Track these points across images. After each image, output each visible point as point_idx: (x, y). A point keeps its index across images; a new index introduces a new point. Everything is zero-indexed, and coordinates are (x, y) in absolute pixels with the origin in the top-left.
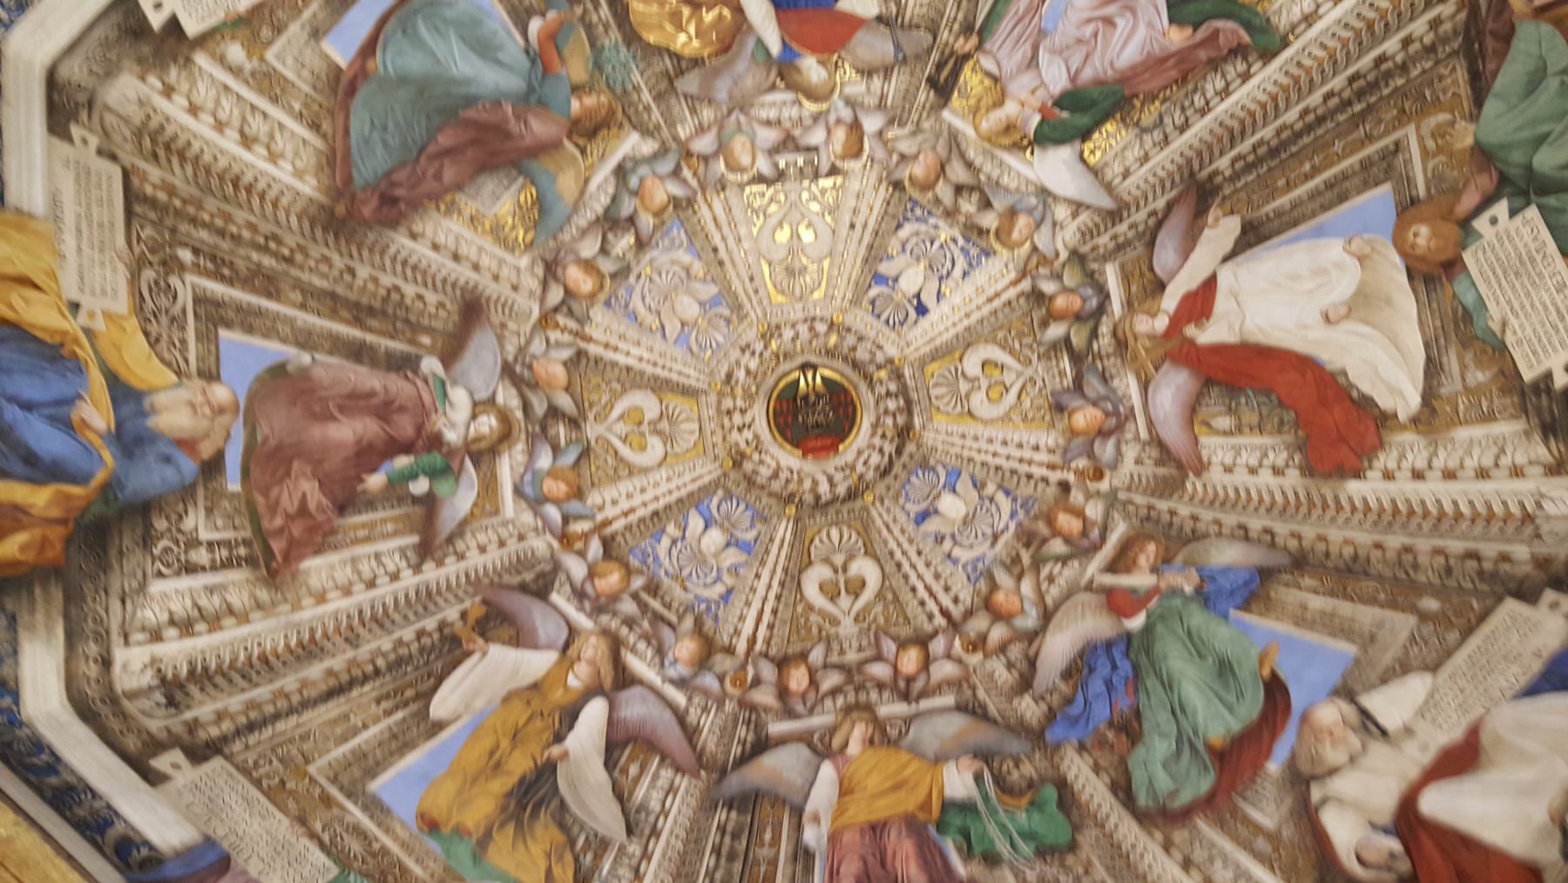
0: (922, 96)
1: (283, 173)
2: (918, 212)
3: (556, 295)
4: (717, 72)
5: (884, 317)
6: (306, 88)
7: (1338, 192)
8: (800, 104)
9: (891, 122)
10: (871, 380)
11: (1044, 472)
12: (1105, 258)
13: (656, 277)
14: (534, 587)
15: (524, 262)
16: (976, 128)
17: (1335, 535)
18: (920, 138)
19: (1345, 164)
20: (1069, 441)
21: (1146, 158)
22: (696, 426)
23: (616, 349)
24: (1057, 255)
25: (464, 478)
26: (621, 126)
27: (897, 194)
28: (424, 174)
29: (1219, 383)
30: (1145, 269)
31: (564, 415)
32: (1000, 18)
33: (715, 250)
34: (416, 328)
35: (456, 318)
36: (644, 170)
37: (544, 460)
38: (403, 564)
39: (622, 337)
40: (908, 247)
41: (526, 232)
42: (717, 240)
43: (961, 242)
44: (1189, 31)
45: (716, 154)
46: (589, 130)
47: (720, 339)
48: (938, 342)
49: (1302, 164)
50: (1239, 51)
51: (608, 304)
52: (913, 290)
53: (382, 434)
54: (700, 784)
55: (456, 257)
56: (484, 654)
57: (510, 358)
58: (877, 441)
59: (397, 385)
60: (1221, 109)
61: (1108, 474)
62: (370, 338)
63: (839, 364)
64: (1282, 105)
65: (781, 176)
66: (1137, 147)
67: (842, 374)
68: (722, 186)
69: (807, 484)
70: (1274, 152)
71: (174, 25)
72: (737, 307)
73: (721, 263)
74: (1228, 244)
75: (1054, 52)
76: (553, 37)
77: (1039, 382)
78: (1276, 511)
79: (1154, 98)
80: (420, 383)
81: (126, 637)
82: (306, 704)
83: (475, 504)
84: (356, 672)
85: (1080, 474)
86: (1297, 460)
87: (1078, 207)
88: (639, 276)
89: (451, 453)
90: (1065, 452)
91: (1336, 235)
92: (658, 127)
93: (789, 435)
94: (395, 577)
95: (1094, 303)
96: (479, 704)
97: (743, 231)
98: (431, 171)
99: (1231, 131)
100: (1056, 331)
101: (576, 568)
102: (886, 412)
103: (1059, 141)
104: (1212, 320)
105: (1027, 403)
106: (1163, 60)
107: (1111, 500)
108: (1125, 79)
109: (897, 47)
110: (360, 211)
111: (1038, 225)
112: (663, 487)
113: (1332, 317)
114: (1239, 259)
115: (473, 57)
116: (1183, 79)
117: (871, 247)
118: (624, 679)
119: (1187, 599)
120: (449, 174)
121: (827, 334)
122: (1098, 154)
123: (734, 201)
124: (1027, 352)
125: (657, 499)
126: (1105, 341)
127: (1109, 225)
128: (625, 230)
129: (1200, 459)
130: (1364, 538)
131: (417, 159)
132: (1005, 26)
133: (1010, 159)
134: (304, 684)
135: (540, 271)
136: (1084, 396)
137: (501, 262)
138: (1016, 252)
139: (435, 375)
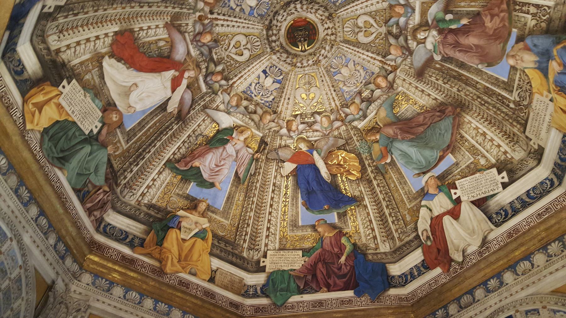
0: (269, 140)
1: (475, 123)
2: (267, 104)
3: (390, 77)
4: (333, 145)
5: (277, 69)
6: (462, 148)
7: (141, 125)
8: (306, 136)
9: (278, 132)
10: (281, 47)
11: (219, 17)
13: (356, 82)
15: (400, 89)
16: (252, 131)
17: (119, 10)
18: (268, 127)
20: (211, 29)
21: (199, 126)
22: (345, 29)
23: (371, 57)
24: (222, 93)
25: (432, 17)
27: (275, 109)
28: (429, 119)
29: (165, 57)
30: (194, 92)
31: (393, 36)
33: (335, 91)
34: (439, 70)
35: (426, 72)
36: (357, 116)
37: (402, 20)
40: (270, 93)
41: (398, 99)
42: (334, 94)
43: (253, 95)
45: (334, 121)
46: (374, 129)
47: (334, 60)
48: (258, 61)
51: (373, 73)
52: (267, 78)
53: (459, 37)
55: (423, 91)
57: (409, 57)
58: (279, 24)
59: (451, 53)
61: (197, 19)
62: (457, 69)
63: (293, 52)
64: (162, 147)
65: (313, 114)
66: (202, 129)
69: (305, 7)
71: (500, 172)
72: (328, 71)
73: (333, 86)
74: (170, 103)
75: (231, 156)
76: (383, 157)
78: (140, 13)
79: (199, 145)
80: (442, 52)
85: (207, 18)
87: (217, 109)
88: (361, 83)
89: (435, 27)
92: (352, 129)
93: (311, 26)
95: (208, 79)
97: (325, 97)
98: (427, 120)
99: (175, 137)
100: (219, 68)
102: (276, 35)
103: (226, 129)
104: (170, 78)
105: (227, 41)
107: (195, 10)
108: (209, 150)
109: (278, 154)
110: (452, 109)
111: (229, 102)
113: (134, 86)
114: (166, 99)
115: (409, 153)
116: (192, 151)
117: (283, 92)
120: (421, 118)
122: (213, 126)
124: (228, 60)
126: (203, 66)
129: (167, 29)
131: (431, 123)
132: (247, 162)
133: (241, 123)
135: (395, 85)
136: (208, 46)
137: (408, 89)
139: (437, 54)
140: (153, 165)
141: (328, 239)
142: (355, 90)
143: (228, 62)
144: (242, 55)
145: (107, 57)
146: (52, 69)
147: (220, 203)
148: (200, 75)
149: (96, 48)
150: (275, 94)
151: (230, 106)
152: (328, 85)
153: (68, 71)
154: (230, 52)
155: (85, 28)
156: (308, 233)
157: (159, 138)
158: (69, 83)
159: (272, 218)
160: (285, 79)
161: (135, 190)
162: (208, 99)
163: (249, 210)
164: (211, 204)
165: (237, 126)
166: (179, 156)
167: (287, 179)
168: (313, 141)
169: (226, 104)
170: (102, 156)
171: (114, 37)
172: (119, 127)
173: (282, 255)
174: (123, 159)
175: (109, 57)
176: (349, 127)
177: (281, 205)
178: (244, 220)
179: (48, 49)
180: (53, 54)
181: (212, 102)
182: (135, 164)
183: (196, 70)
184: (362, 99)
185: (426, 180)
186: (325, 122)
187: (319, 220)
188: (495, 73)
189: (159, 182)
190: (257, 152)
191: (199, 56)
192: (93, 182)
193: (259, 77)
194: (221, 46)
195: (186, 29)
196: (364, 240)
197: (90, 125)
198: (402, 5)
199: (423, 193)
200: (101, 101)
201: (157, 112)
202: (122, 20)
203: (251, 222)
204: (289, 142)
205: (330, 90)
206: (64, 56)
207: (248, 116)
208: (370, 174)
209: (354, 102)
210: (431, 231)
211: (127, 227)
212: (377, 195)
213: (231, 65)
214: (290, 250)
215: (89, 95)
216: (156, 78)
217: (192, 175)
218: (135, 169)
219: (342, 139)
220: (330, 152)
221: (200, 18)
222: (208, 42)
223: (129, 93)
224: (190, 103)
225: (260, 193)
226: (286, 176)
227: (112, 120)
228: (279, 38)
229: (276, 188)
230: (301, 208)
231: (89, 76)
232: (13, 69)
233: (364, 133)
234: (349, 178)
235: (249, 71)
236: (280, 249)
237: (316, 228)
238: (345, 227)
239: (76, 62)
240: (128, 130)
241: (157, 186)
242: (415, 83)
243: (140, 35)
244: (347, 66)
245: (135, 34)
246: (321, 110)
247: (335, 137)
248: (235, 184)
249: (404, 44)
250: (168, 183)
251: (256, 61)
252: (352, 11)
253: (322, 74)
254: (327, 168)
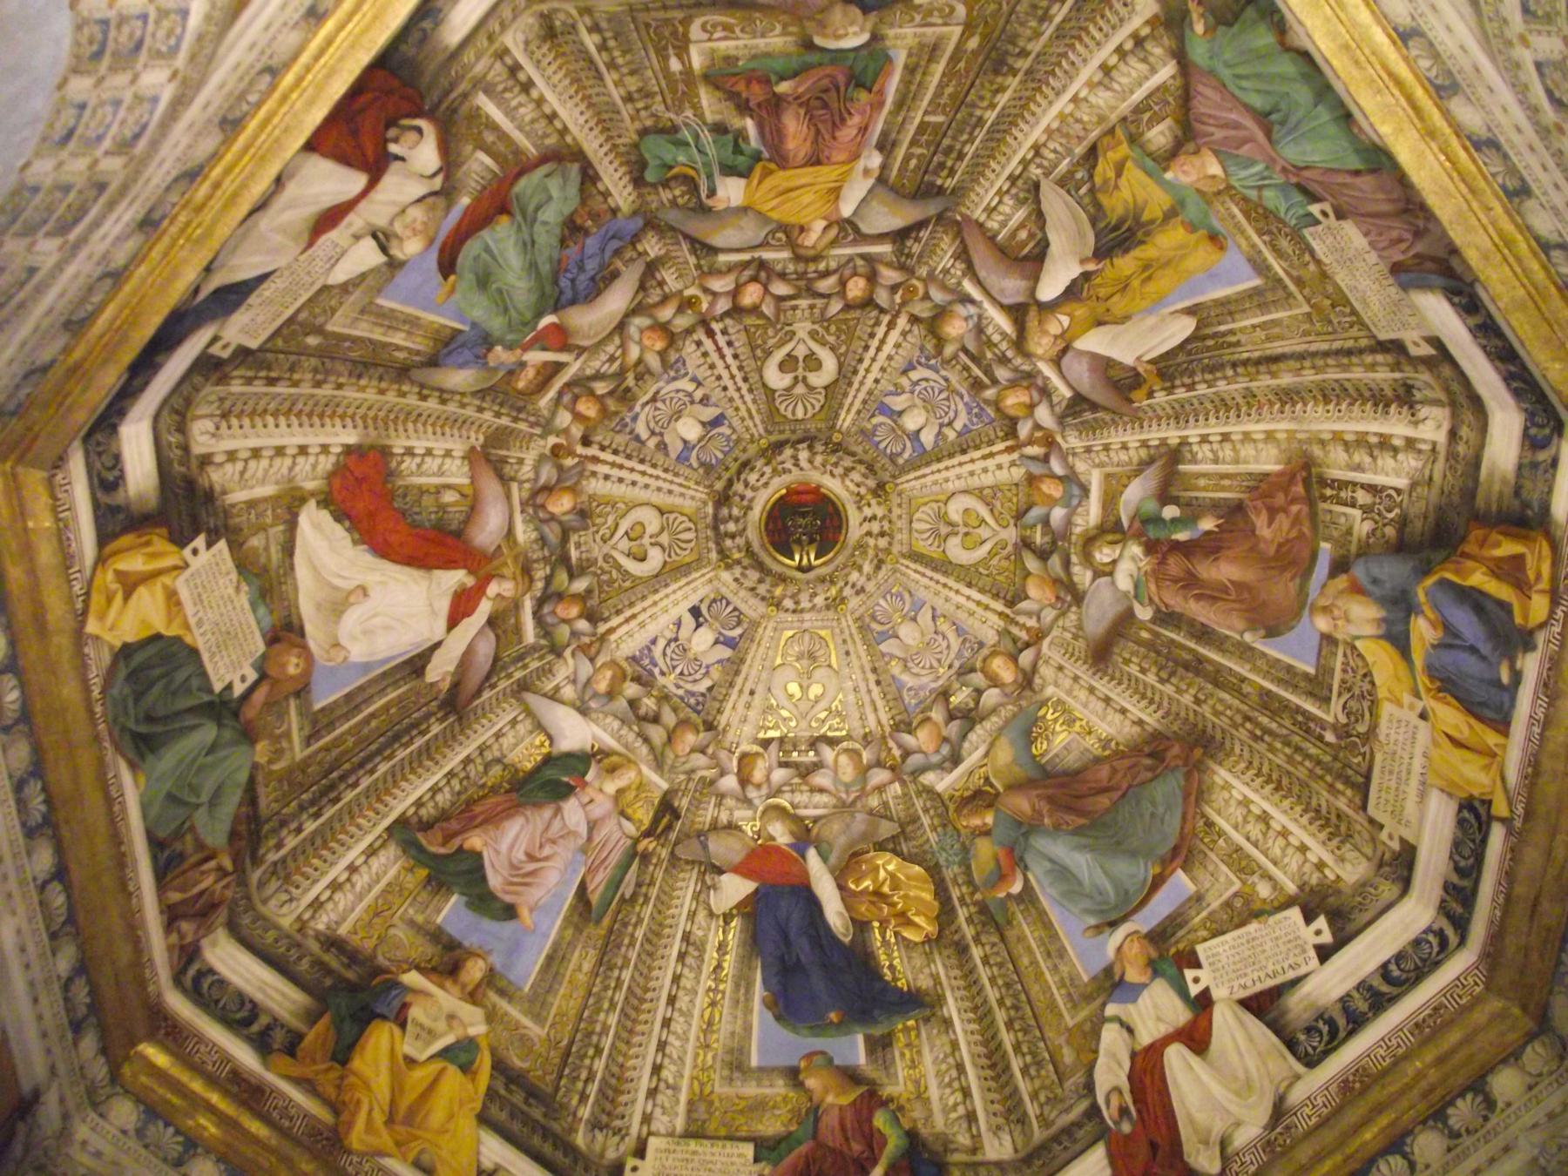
2: (692, 701)
3: (1026, 658)
4: (864, 837)
7: (353, 702)
8: (792, 804)
9: (712, 782)
12: (534, 648)
13: (935, 664)
14: (1086, 406)
15: (1050, 691)
16: (640, 772)
18: (688, 767)
19: (346, 726)
20: (576, 484)
21: (498, 735)
22: (915, 525)
23: (979, 603)
24: (573, 654)
25: (1131, 511)
26: (951, 798)
31: (1034, 552)
32: (617, 866)
33: (878, 683)
34: (1150, 646)
35: (1116, 650)
36: (935, 759)
37: (1058, 514)
38: (1195, 448)
39: (972, 614)
40: (703, 671)
41: (1044, 717)
42: (876, 690)
43: (656, 671)
44: (467, 846)
45: (870, 767)
46: (979, 798)
47: (882, 602)
48: (683, 581)
49: (378, 728)
50: (426, 826)
51: (981, 645)
52: (701, 630)
54: (963, 210)
55: (1107, 700)
56: (1138, 359)
57: (1074, 609)
59: (1176, 601)
60: (437, 777)
61: (547, 452)
63: (776, 568)
64: (389, 778)
65: (814, 743)
67: (775, 559)
68: (867, 739)
70: (397, 737)
72: (863, 628)
73: (874, 670)
75: (572, 834)
80: (1156, 599)
81: (1434, 450)
82: (1301, 357)
83: (1126, 486)
84: (1252, 369)
87: (554, 696)
88: (950, 667)
89: (1139, 536)
92: (919, 794)
94: (1204, 439)
95: (546, 609)
96: (1151, 320)
97: (851, 698)
98: (1119, 776)
99: (430, 758)
100: (580, 585)
101: (1043, 415)
103: (569, 755)
106: (486, 821)
109: (705, 847)
111: (589, 681)
112: (953, 474)
113: (360, 592)
116: (470, 803)
117: (737, 673)
118: (1017, 312)
119: (500, 341)
121: (784, 597)
122: (537, 742)
123: (857, 724)
124: (606, 566)
125: (961, 464)
128: (956, 708)
130: (350, 394)
132: (615, 858)
133: (611, 743)
134: (1298, 372)
135: (1037, 681)
137: (1069, 692)
140: (359, 827)
141: (836, 1112)
142: (934, 685)
143: (604, 572)
144: (643, 560)
145: (312, 503)
147: (527, 970)
148: (528, 596)
150: (716, 674)
152: (862, 668)
153: (216, 514)
154: (614, 547)
155: (282, 420)
156: (776, 1090)
158: (209, 545)
159: (672, 1039)
160: (749, 636)
161: (297, 887)
162: (534, 665)
163: (606, 1005)
164: (498, 967)
165: (600, 751)
166: (432, 811)
167: (726, 923)
168: (808, 818)
169: (580, 686)
170: (237, 764)
172: (297, 694)
173: (694, 1153)
174: (286, 787)
176: (912, 787)
177: (701, 1000)
178: (589, 1034)
179: (186, 448)
180: (194, 464)
182: (312, 810)
184: (949, 711)
185: (1118, 943)
186: (847, 771)
187: (809, 1056)
188: (1285, 652)
189: (366, 878)
190: (647, 834)
192: (201, 830)
193: (679, 624)
196: (939, 1122)
198: (1059, 478)
199: (1112, 984)
202: (370, 422)
203: (607, 1043)
204: (741, 814)
205: (866, 680)
206: (217, 477)
207: (635, 728)
208: (964, 925)
209: (928, 719)
210: (1132, 1092)
211: (260, 989)
212: (981, 989)
213: (611, 582)
214: (718, 1138)
217: (459, 874)
218: (310, 826)
219: (891, 819)
220: (855, 855)
222: (565, 514)
224: (487, 667)
225: (644, 957)
226: (725, 915)
228: (744, 529)
229: (691, 949)
230: (759, 1015)
232: (99, 475)
233: (952, 807)
234: (905, 934)
235: (655, 603)
236: (689, 1135)
237: (801, 1077)
238: (885, 1080)
239: (238, 496)
240: (317, 706)
241: (358, 888)
242: (1087, 677)
244: (914, 619)
246: (837, 734)
247: (871, 813)
248: (576, 919)
249: (1062, 574)
250: (389, 884)
251: (676, 580)
252: (935, 483)
253: (846, 635)
254: (843, 899)
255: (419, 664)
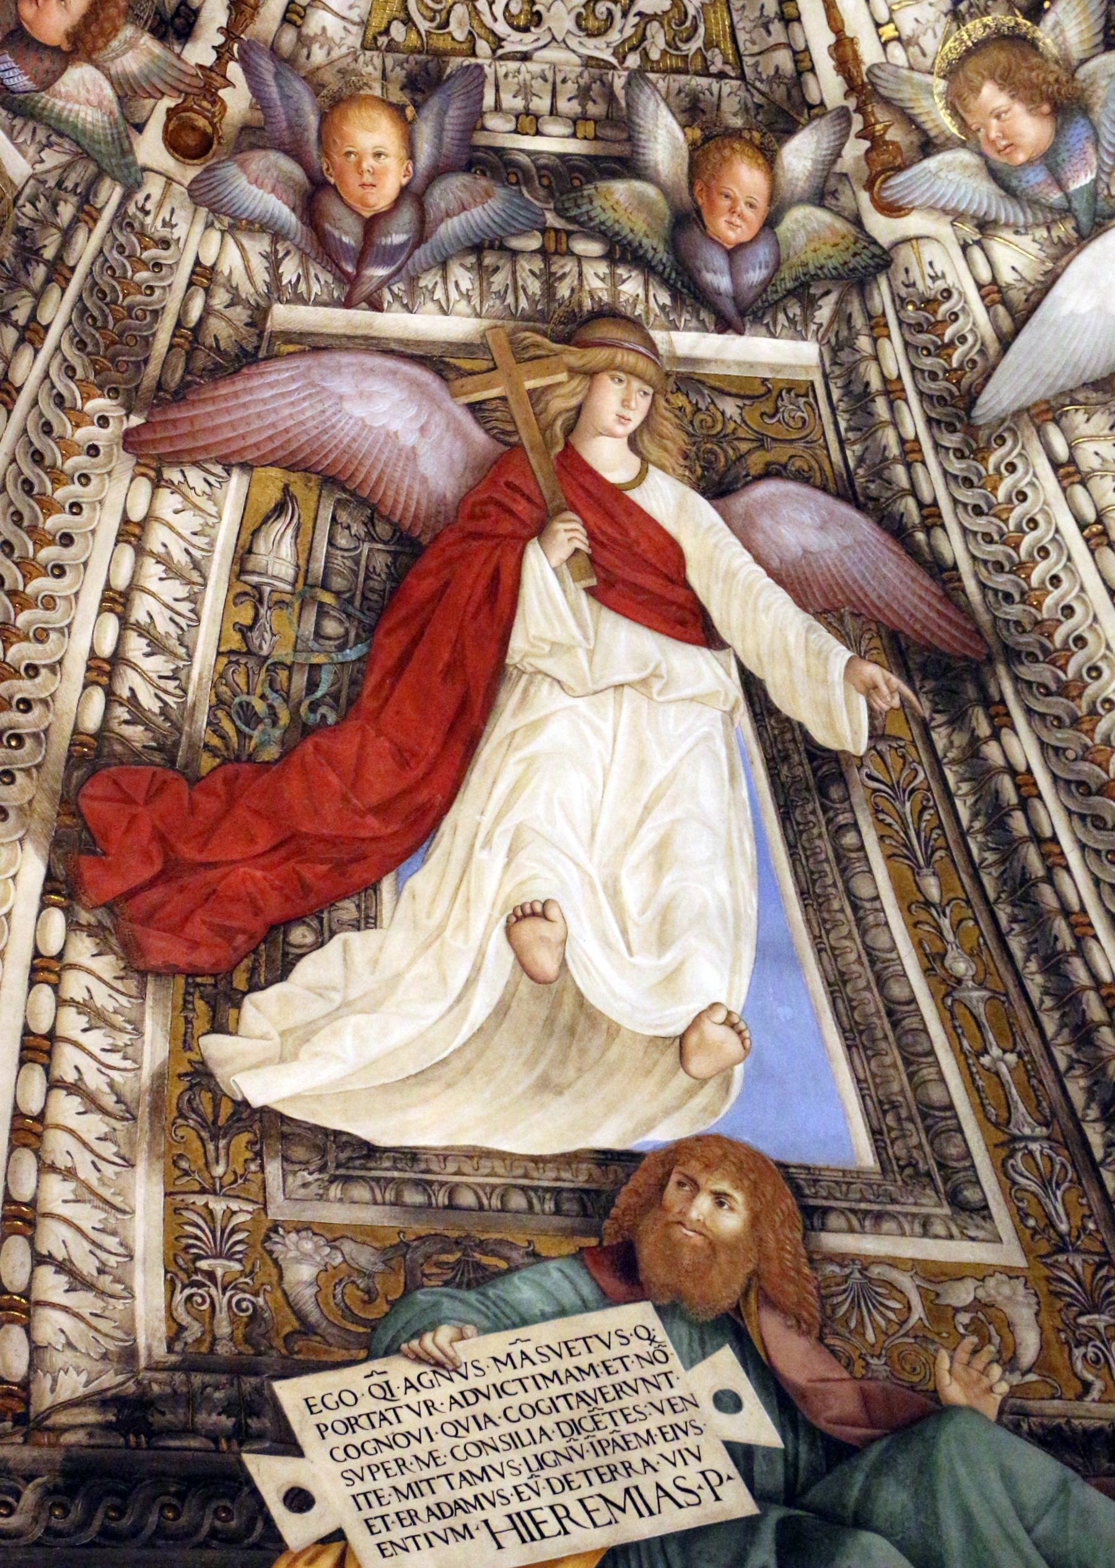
24: (892, 210)
29: (398, 576)
30: (779, 454)
77: (516, 42)
86: (129, 731)
90: (286, 62)
91: (755, 991)
95: (720, 281)
104: (584, 602)
111: (995, 174)
113: (528, 930)
114: (744, 720)
127: (929, 386)
129: (177, 459)
136: (438, 172)
138: (940, 85)
143: (639, 43)
145: (214, 1046)
146: (126, 1522)
148: (658, 336)
149: (109, 1101)
151: (1036, 179)
153: (192, 1401)
157: (1060, 926)
158: (288, 1445)
169: (1006, 210)
171: (85, 917)
175: (218, 1027)
181: (936, 326)
183: (599, 356)
191: (499, 280)
194: (483, 47)
195: (234, 291)
197: (689, 1441)
200: (536, 1257)
201: (825, 847)
215: (445, 1333)
216: (535, 727)
221: (191, 140)
223: (568, 1000)
224: (863, 526)
227: (733, 1246)
231: (304, 1257)
240: (865, 1156)
243: (148, 701)
245: (124, 740)
255: (804, 770)
